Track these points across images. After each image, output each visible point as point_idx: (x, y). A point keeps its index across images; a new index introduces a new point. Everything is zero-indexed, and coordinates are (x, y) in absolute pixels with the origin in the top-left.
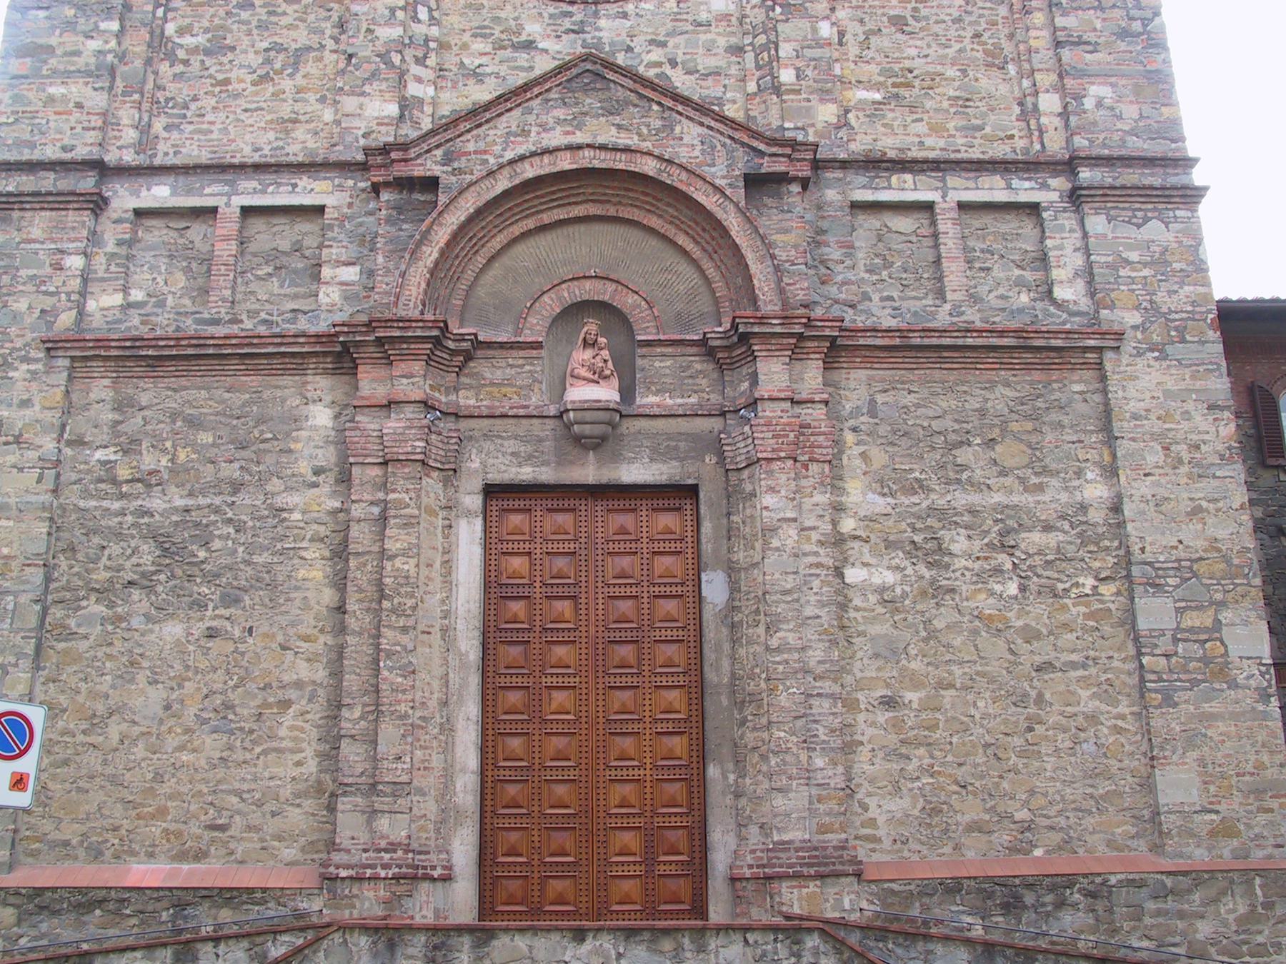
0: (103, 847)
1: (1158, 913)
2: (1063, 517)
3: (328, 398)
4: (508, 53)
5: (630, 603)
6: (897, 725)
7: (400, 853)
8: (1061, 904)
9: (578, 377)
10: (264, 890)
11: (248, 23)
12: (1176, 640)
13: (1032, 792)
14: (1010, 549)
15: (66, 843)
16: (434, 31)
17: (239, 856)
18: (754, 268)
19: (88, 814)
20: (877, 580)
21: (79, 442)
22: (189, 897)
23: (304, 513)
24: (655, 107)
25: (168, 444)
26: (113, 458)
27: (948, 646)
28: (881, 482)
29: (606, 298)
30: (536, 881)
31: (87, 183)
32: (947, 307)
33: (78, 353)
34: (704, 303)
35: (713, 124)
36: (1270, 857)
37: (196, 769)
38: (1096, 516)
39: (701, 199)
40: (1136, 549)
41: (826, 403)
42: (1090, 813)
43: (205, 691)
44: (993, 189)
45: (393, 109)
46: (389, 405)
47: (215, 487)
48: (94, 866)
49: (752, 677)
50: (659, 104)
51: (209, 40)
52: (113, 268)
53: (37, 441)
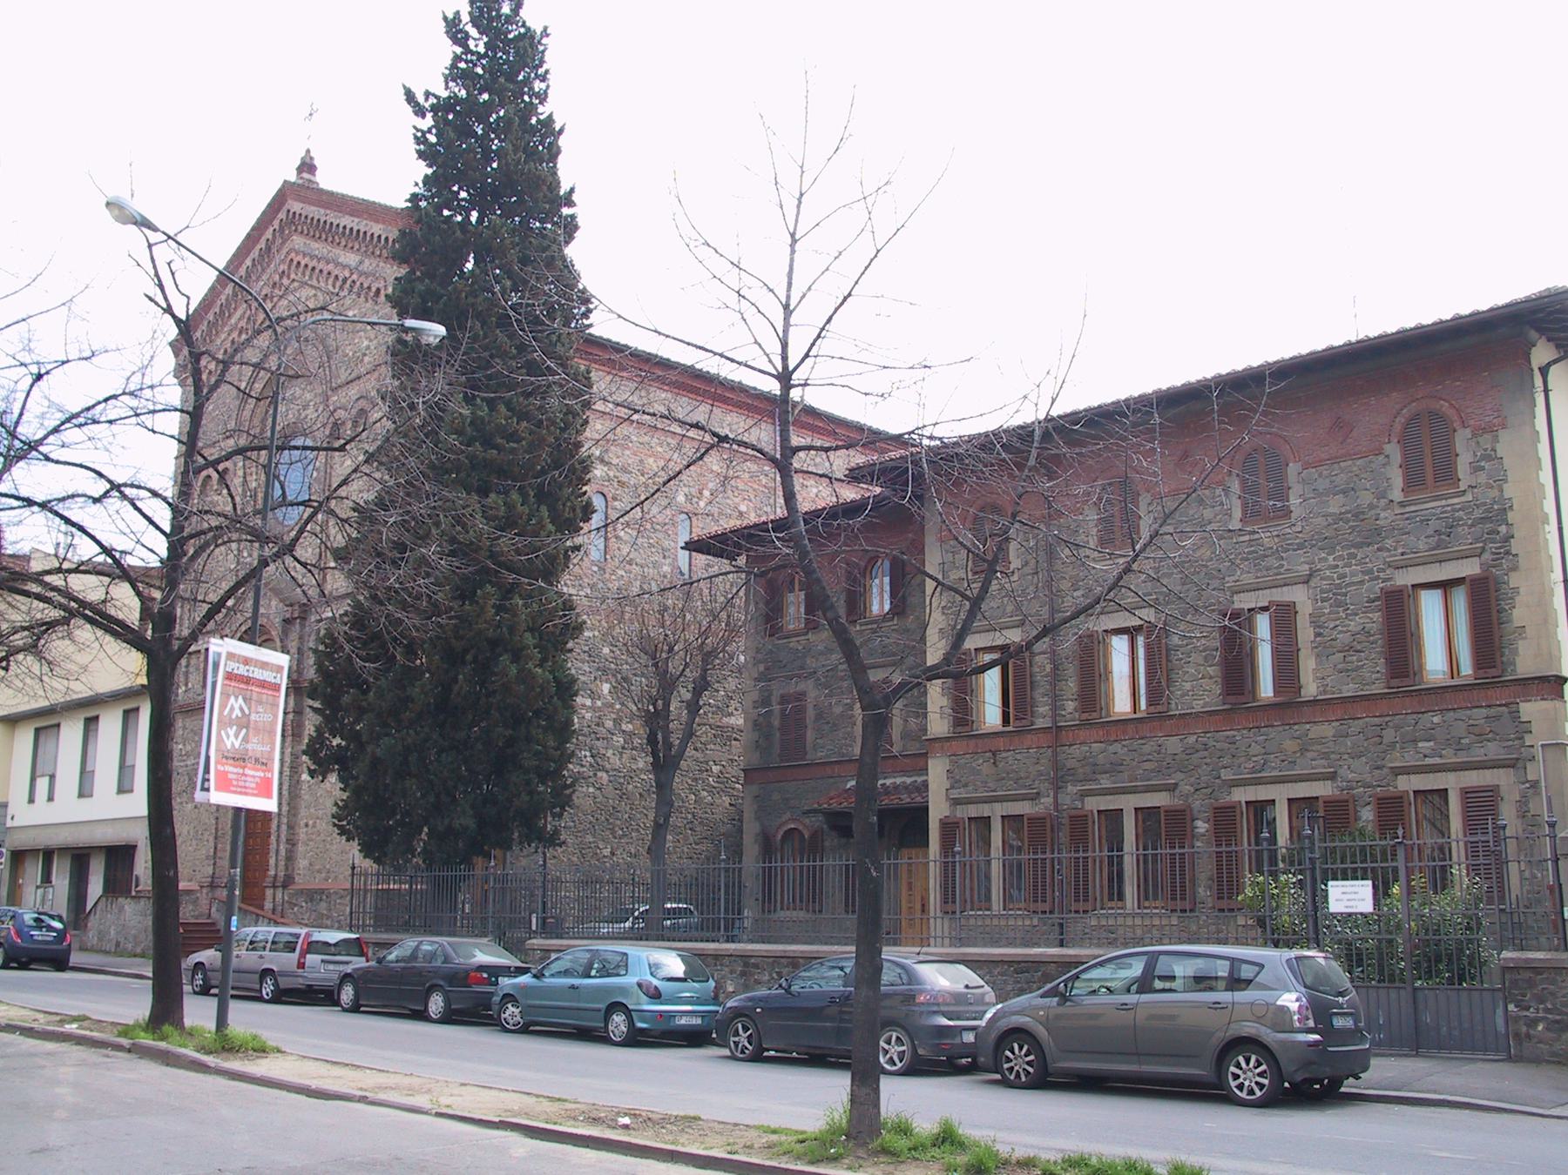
8: (321, 900)
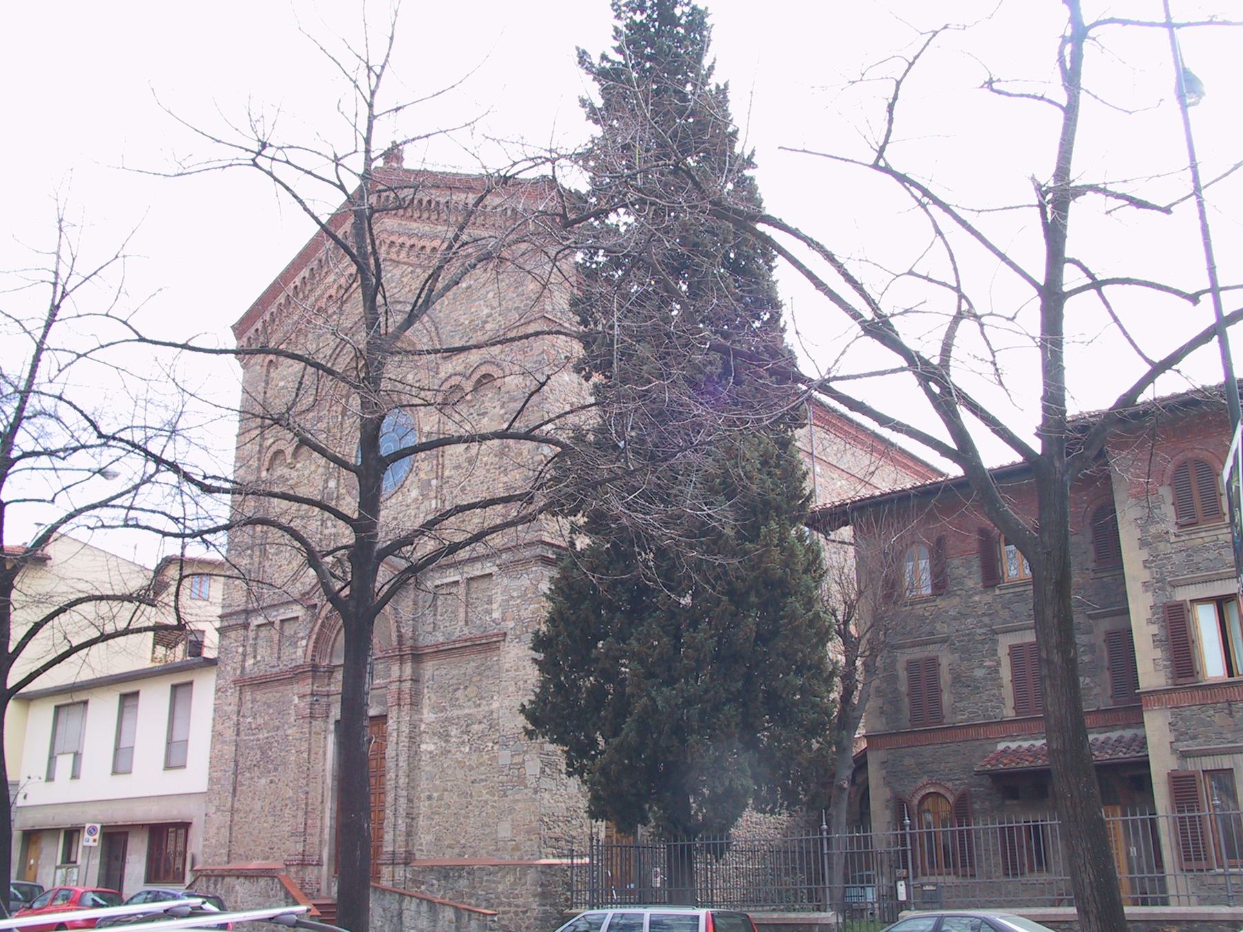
1: (487, 881)
8: (460, 877)
12: (510, 769)
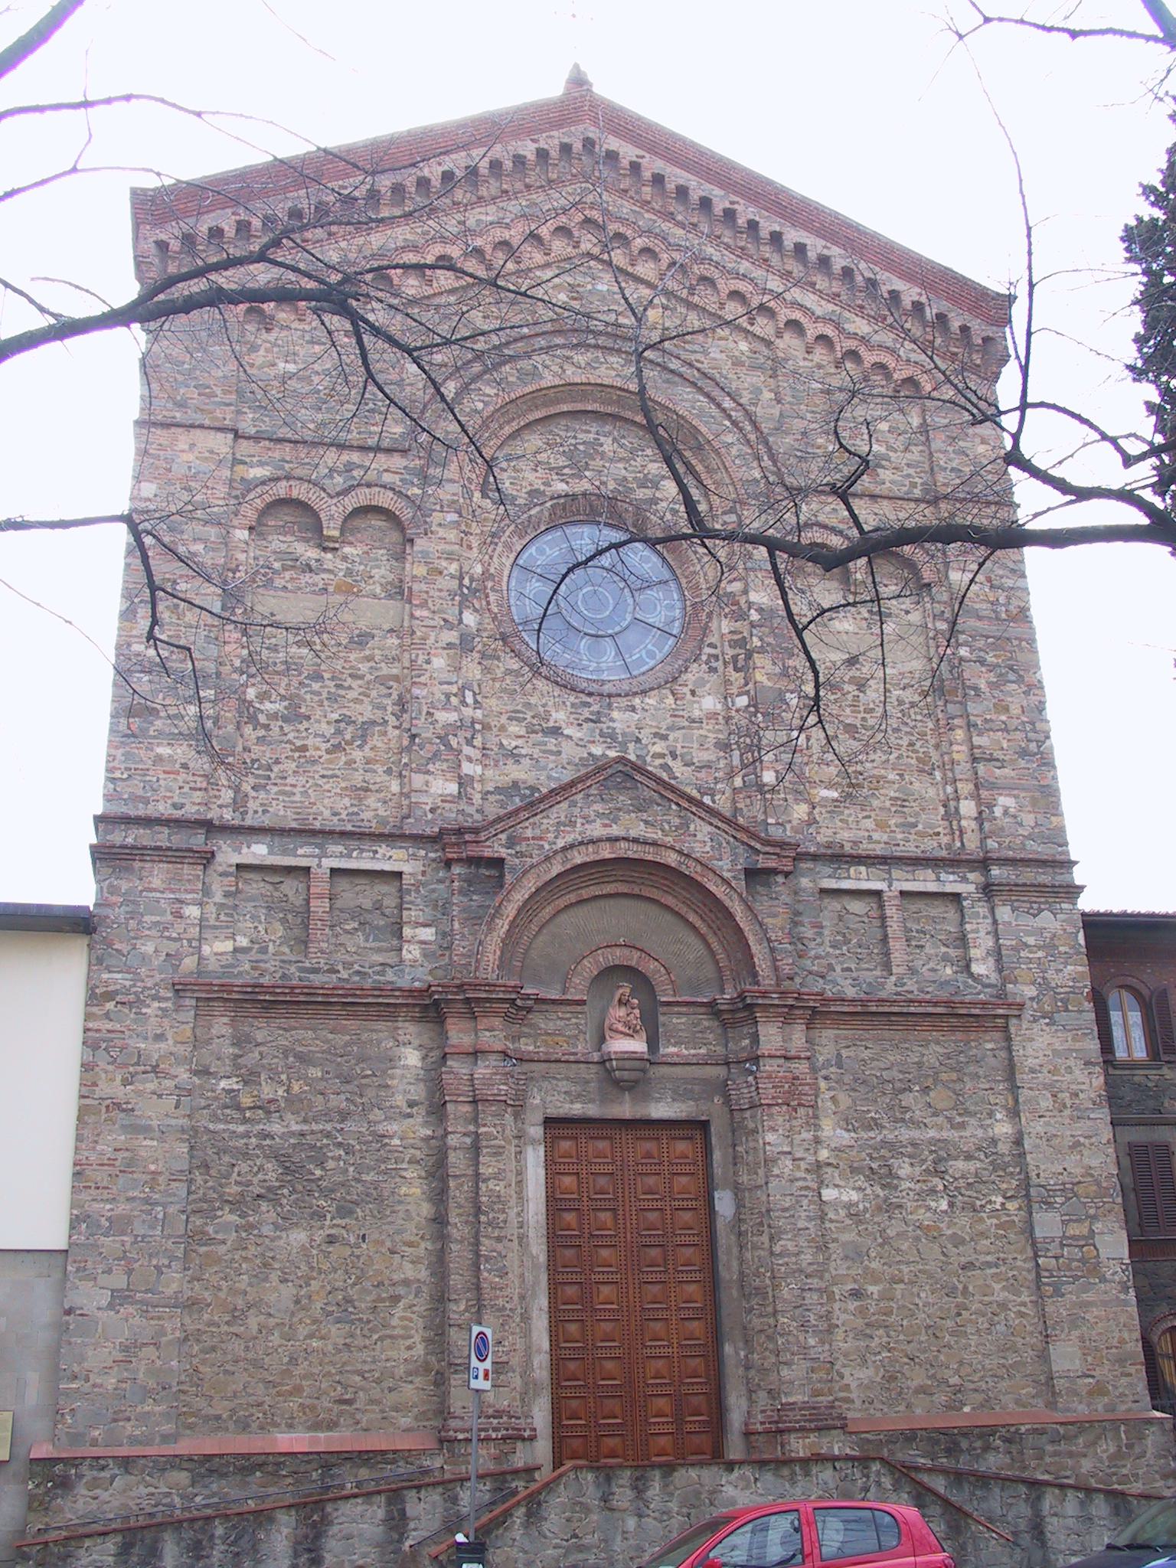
0: (249, 1420)
1: (1056, 1454)
2: (979, 1149)
3: (416, 1042)
4: (539, 737)
5: (656, 1214)
6: (862, 1311)
7: (505, 1419)
8: (987, 1448)
9: (617, 1031)
10: (395, 1452)
11: (319, 694)
12: (1062, 1246)
13: (961, 1363)
14: (941, 1174)
15: (218, 1418)
16: (479, 714)
17: (364, 1424)
18: (755, 948)
19: (235, 1393)
20: (845, 1198)
21: (204, 1072)
22: (333, 1460)
23: (402, 1139)
24: (674, 807)
25: (284, 1077)
26: (236, 1087)
27: (898, 1250)
28: (847, 1120)
29: (633, 963)
30: (593, 1439)
31: (198, 840)
32: (893, 978)
33: (204, 995)
34: (709, 971)
35: (720, 824)
36: (1129, 1410)
37: (324, 1354)
38: (1003, 1148)
39: (713, 888)
40: (1033, 1175)
41: (808, 1058)
42: (1003, 1378)
43: (329, 1288)
44: (925, 881)
45: (453, 788)
46: (476, 1054)
47: (326, 1115)
48: (244, 1437)
49: (757, 1274)
50: (677, 804)
51: (286, 708)
52: (222, 917)
53: (173, 1071)
